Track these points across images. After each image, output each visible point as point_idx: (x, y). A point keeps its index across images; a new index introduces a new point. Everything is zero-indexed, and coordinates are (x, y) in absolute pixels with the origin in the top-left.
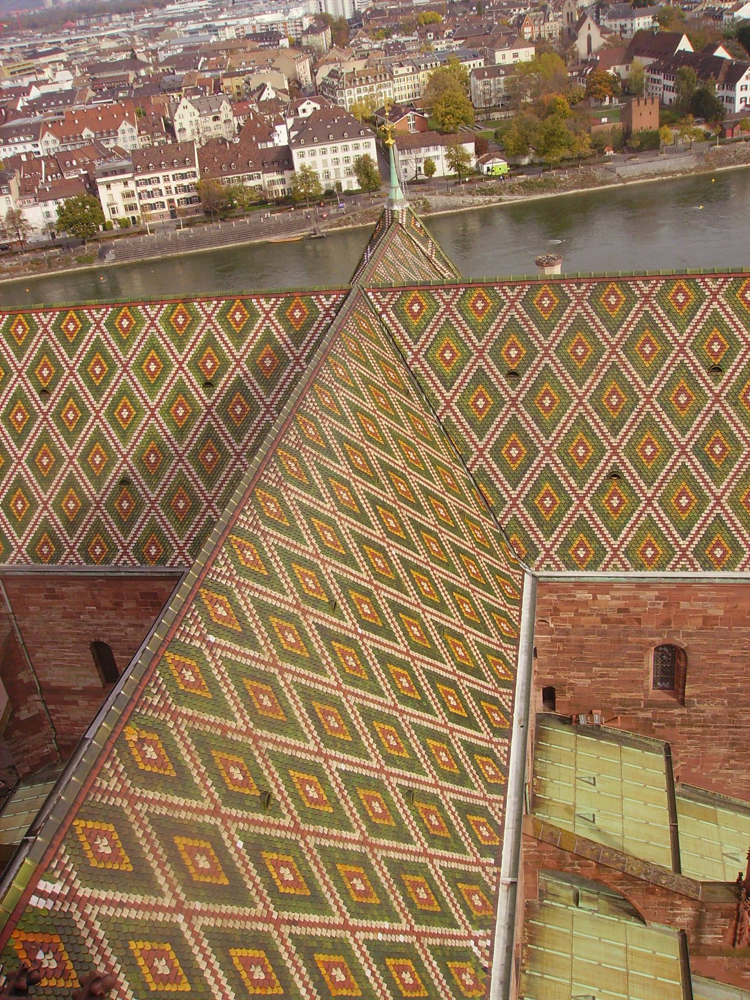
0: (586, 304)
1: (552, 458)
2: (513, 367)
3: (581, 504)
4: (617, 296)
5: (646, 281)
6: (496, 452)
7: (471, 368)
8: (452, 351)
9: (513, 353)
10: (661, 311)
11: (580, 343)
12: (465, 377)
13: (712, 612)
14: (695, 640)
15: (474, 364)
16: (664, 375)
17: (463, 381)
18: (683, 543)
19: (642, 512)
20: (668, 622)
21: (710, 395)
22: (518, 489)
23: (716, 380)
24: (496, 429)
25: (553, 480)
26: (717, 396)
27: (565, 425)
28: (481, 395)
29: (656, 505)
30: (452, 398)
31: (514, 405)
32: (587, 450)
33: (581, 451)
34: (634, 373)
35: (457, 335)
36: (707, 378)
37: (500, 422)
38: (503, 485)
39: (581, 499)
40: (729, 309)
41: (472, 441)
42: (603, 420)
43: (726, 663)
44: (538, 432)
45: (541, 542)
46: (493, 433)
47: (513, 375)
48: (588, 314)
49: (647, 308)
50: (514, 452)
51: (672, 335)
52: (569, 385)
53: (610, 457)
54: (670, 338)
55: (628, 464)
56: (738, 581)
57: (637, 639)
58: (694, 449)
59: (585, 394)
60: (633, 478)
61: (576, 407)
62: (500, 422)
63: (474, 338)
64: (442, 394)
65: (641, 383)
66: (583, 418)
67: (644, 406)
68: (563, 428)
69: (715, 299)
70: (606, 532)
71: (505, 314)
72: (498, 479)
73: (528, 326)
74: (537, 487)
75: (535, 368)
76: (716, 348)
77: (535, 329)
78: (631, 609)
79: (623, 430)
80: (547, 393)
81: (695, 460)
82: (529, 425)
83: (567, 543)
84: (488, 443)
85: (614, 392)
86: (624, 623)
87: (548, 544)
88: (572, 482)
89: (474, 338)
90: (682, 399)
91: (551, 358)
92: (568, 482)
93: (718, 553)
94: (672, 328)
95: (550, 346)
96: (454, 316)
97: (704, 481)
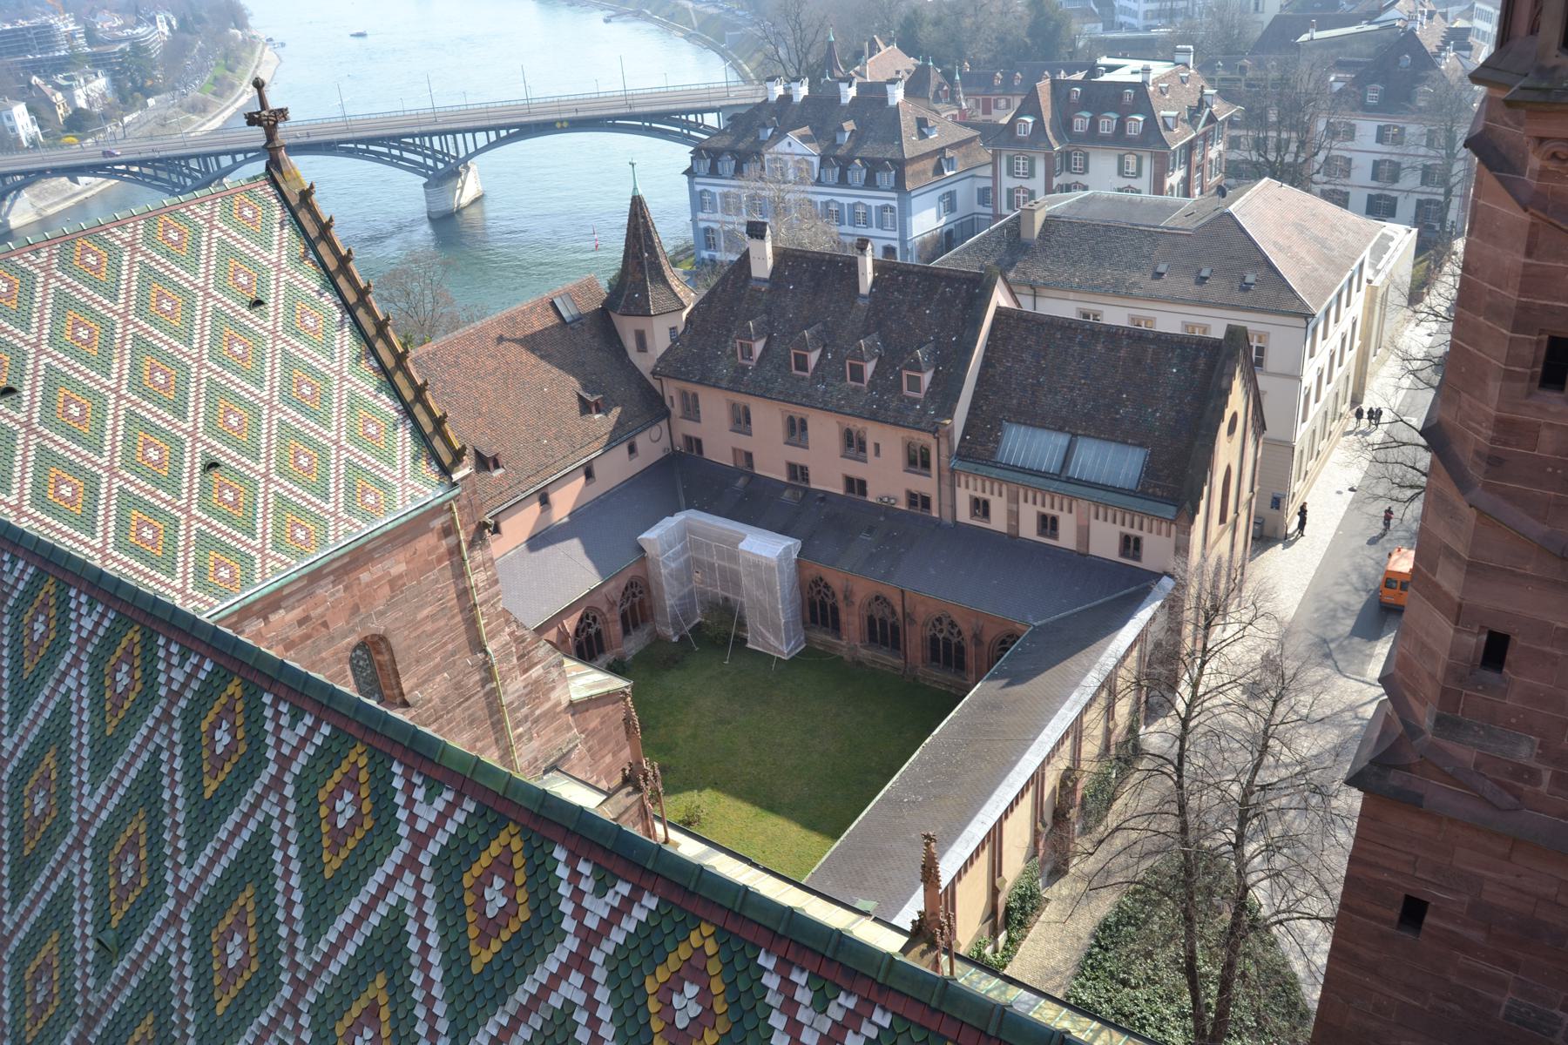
0: (59, 274)
1: (121, 478)
3: (190, 516)
5: (123, 227)
6: (40, 500)
10: (158, 257)
11: (77, 324)
13: (395, 571)
14: (391, 615)
18: (330, 507)
20: (355, 610)
21: (266, 334)
23: (264, 316)
24: (23, 471)
25: (137, 502)
26: (274, 332)
27: (114, 430)
29: (276, 478)
32: (160, 451)
33: (153, 455)
34: (166, 338)
36: (252, 316)
38: (75, 539)
39: (187, 511)
40: (234, 234)
42: (160, 406)
43: (429, 627)
44: (84, 452)
45: (167, 586)
46: (22, 478)
48: (69, 286)
49: (139, 258)
52: (92, 379)
54: (186, 285)
55: (219, 446)
56: (410, 516)
57: (332, 650)
58: (282, 399)
59: (119, 383)
60: (234, 459)
65: (181, 347)
66: (133, 413)
67: (199, 373)
68: (114, 435)
69: (212, 227)
70: (239, 535)
74: (122, 524)
76: (243, 280)
78: (313, 614)
80: (68, 400)
81: (289, 411)
83: (200, 571)
84: (21, 495)
85: (153, 369)
86: (308, 637)
87: (178, 583)
88: (164, 495)
91: (49, 355)
93: (370, 499)
94: (182, 272)
97: (312, 430)
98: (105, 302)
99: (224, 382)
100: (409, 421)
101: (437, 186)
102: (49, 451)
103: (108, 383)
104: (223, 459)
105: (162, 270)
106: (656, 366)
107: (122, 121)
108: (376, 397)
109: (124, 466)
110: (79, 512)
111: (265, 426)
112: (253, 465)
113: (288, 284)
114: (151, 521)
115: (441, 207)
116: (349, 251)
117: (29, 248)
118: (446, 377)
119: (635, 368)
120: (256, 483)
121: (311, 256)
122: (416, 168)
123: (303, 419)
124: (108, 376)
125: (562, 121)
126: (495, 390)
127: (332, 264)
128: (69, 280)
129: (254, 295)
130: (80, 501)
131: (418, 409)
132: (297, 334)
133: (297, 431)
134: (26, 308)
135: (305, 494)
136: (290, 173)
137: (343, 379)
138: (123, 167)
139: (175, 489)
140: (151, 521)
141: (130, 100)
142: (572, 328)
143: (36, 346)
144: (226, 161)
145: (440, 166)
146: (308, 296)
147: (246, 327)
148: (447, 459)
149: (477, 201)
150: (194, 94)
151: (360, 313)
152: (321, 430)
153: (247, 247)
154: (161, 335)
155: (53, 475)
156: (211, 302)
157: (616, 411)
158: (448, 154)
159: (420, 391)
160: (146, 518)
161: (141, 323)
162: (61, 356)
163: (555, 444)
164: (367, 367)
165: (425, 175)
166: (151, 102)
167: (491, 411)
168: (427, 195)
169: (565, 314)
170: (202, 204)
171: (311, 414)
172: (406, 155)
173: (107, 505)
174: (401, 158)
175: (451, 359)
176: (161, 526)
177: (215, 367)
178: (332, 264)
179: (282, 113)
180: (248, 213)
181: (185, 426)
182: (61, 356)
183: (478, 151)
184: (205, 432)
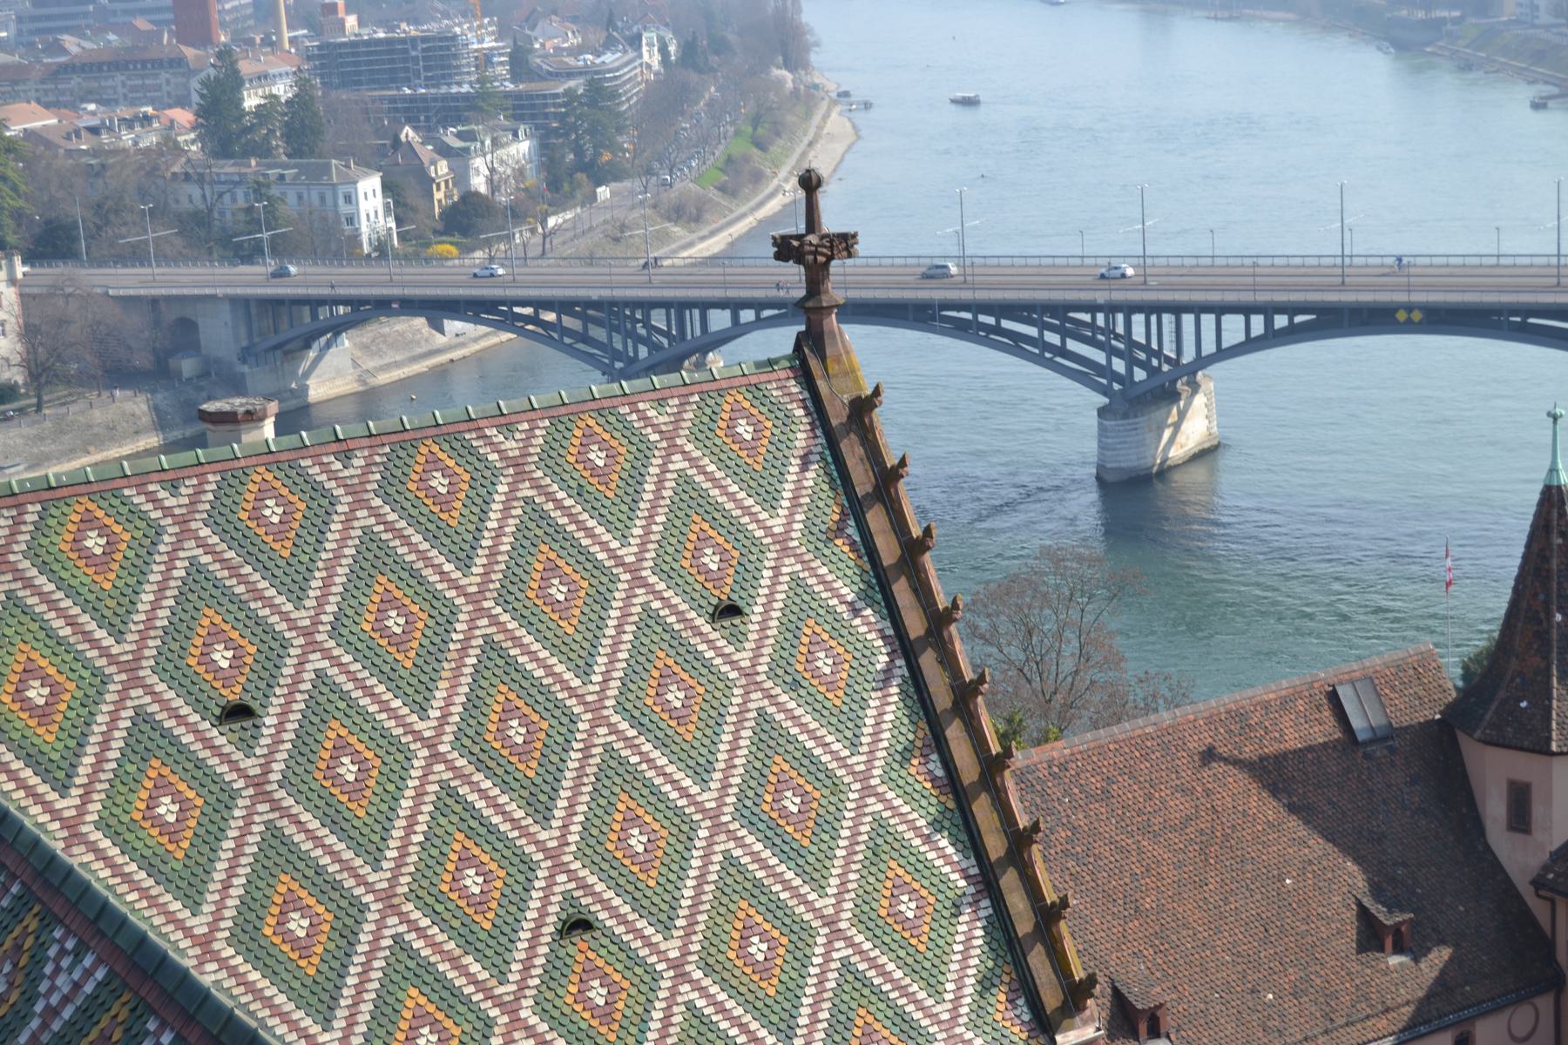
0: (377, 502)
1: (404, 918)
2: (233, 695)
4: (445, 472)
5: (508, 428)
6: (247, 936)
7: (114, 719)
8: (45, 680)
9: (222, 658)
10: (561, 495)
11: (388, 602)
12: (105, 744)
15: (120, 704)
16: (616, 644)
17: (100, 760)
19: (671, 1000)
22: (339, 1024)
23: (737, 638)
24: (231, 872)
25: (422, 974)
26: (749, 674)
28: (162, 787)
29: (698, 974)
30: (81, 810)
31: (262, 795)
32: (487, 876)
33: (473, 882)
34: (543, 654)
35: (50, 634)
36: (714, 635)
37: (238, 852)
39: (511, 1009)
40: (711, 468)
41: (171, 918)
42: (506, 787)
47: (238, 713)
49: (526, 491)
50: (298, 925)
51: (604, 546)
53: (551, 881)
54: (601, 556)
55: (599, 887)
58: (739, 814)
59: (439, 730)
61: (427, 771)
62: (238, 852)
63: (100, 634)
64: (48, 807)
65: (568, 676)
66: (452, 793)
67: (591, 733)
68: (409, 830)
69: (673, 448)
71: (172, 558)
72: (277, 1012)
73: (243, 581)
75: (293, 688)
76: (711, 561)
77: (263, 584)
79: (562, 803)
80: (341, 748)
81: (750, 839)
82: (318, 841)
88: (475, 968)
89: (100, 634)
90: (675, 697)
91: (327, 654)
92: (463, 970)
94: (600, 530)
95: (316, 622)
96: (28, 584)
97: (787, 886)
98: (448, 567)
99: (634, 759)
100: (985, 903)
101: (1125, 416)
102: (285, 841)
103: (419, 726)
104: (602, 915)
105: (563, 521)
106: (1546, 868)
107: (544, 222)
108: (927, 839)
109: (413, 895)
110: (312, 971)
111: (695, 863)
112: (658, 938)
113: (795, 579)
114: (440, 1016)
115: (1128, 459)
116: (927, 532)
117: (335, 447)
118: (1079, 819)
119: (1497, 866)
120: (656, 977)
121: (851, 530)
122: (1088, 374)
123: (773, 861)
124: (422, 712)
125: (1409, 308)
126: (1179, 865)
127: (888, 550)
128: (392, 517)
129: (725, 593)
130: (319, 949)
131: (1009, 880)
132: (795, 686)
133: (758, 884)
134: (305, 558)
135: (747, 1018)
136: (838, 360)
137: (868, 790)
138: (528, 311)
139: (498, 960)
140: (440, 1016)
141: (566, 186)
142: (1367, 756)
143: (308, 633)
144: (720, 320)
145: (1140, 375)
146: (831, 611)
147: (698, 656)
148: (1051, 998)
149: (1205, 454)
150: (684, 186)
151: (928, 660)
152: (805, 889)
153: (731, 497)
154: (536, 647)
155: (282, 889)
156: (641, 596)
157: (1440, 956)
158: (1158, 354)
159: (1020, 842)
160: (431, 1008)
161: (505, 617)
162: (347, 659)
163: (1290, 1004)
164: (921, 773)
165: (1105, 391)
166: (603, 192)
167: (1161, 909)
168: (1102, 430)
169: (1357, 722)
170: (661, 402)
171: (791, 853)
172: (1072, 345)
173: (367, 967)
174: (1063, 352)
175: (1095, 783)
176: (456, 1031)
177: (624, 726)
178: (888, 550)
179: (844, 243)
180: (744, 430)
181: (543, 836)
182: (347, 659)
183: (1222, 354)
184: (580, 854)
